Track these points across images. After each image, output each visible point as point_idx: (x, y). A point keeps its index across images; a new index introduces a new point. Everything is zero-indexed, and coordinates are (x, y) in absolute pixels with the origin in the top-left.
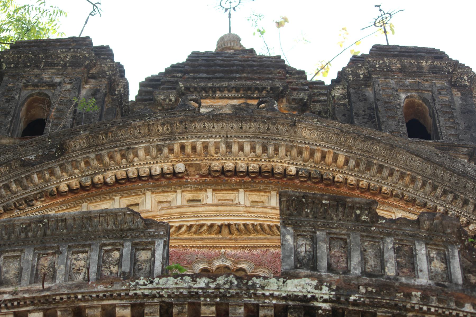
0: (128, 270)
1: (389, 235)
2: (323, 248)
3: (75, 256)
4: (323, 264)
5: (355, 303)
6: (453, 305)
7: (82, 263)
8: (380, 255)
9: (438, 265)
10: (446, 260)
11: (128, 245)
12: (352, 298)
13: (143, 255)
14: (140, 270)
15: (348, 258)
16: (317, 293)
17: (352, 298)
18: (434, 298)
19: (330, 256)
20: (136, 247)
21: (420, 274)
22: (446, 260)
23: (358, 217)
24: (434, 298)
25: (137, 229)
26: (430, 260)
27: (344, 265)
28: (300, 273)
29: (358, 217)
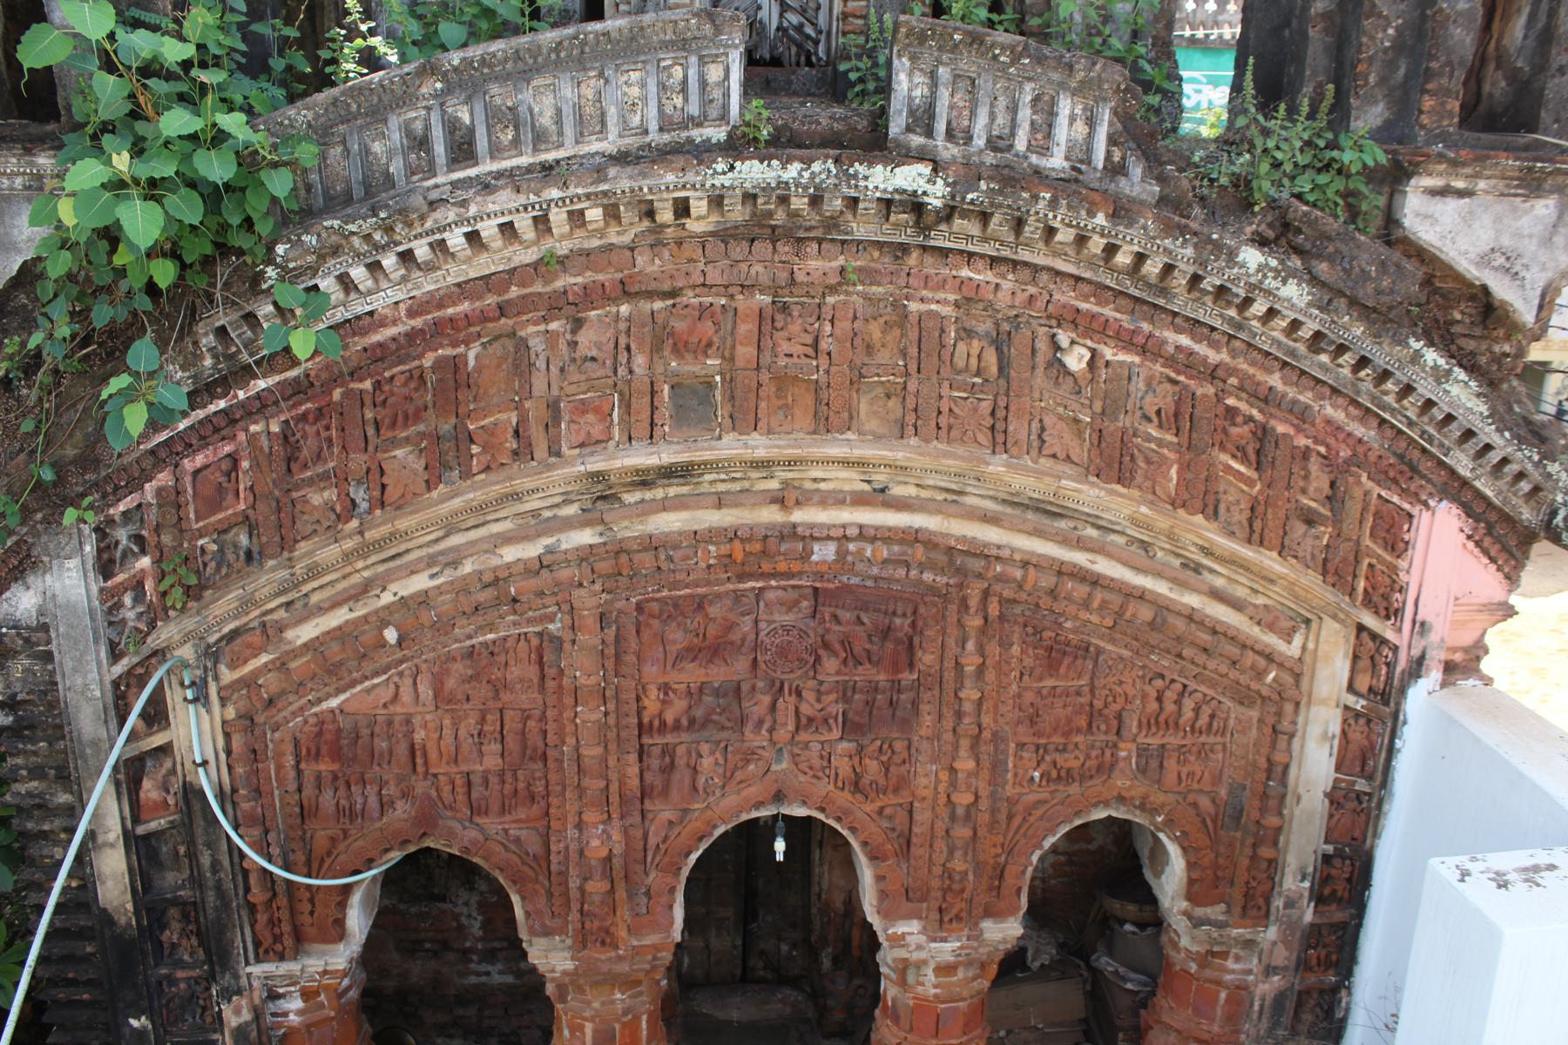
0: (696, 113)
1: (1029, 79)
2: (944, 95)
3: (625, 78)
4: (941, 127)
5: (972, 202)
6: (1083, 213)
7: (635, 91)
8: (1013, 109)
9: (1081, 129)
10: (1091, 122)
11: (693, 59)
12: (970, 196)
13: (714, 73)
14: (711, 101)
15: (973, 114)
16: (929, 188)
17: (970, 196)
18: (1064, 202)
19: (952, 107)
20: (703, 61)
21: (1055, 149)
22: (1091, 122)
23: (995, 57)
24: (1064, 202)
25: (705, 38)
26: (1072, 119)
27: (966, 123)
28: (911, 99)
29: (995, 57)
